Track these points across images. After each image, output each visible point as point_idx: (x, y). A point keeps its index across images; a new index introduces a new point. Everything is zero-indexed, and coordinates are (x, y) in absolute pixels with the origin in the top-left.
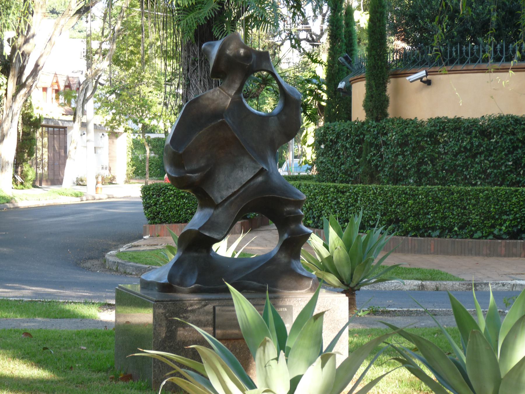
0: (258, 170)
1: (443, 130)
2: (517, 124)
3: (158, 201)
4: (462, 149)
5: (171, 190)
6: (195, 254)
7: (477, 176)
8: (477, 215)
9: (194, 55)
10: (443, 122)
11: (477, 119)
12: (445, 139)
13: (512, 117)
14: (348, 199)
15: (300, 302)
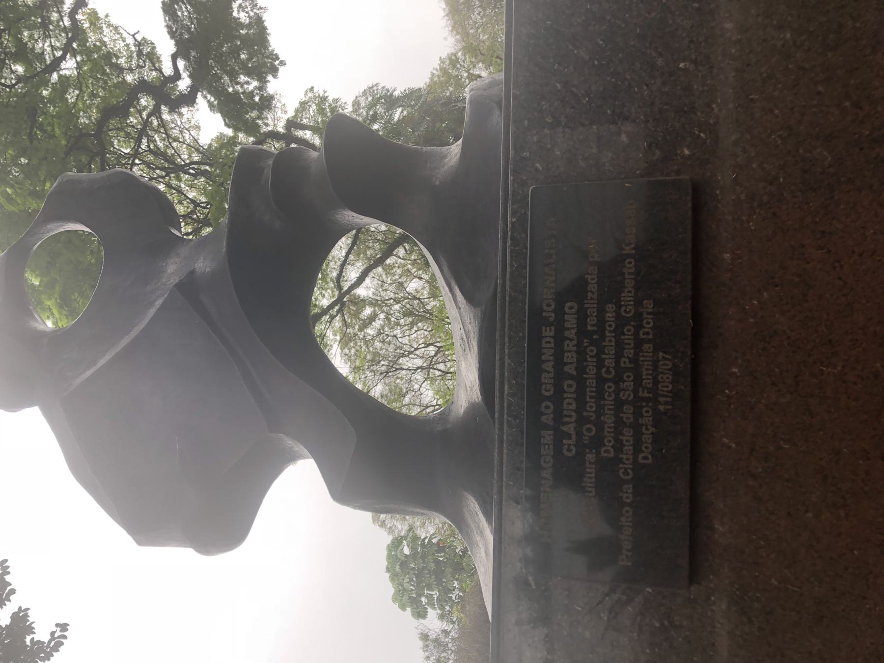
15: (526, 154)
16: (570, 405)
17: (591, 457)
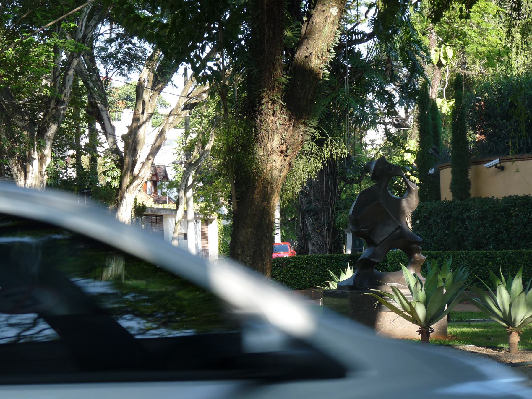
0: (397, 227)
1: (515, 206)
3: (281, 271)
4: (530, 220)
5: (292, 262)
10: (515, 199)
12: (517, 212)
14: (440, 263)
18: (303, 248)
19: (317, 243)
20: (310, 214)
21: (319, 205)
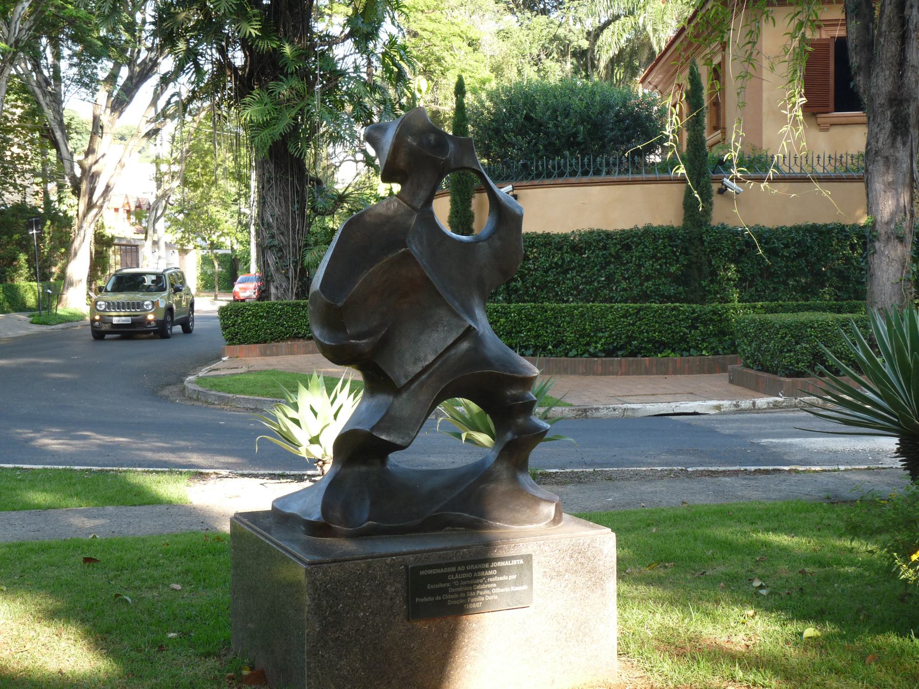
1: (532, 246)
2: (608, 238)
3: (236, 321)
5: (250, 310)
6: (363, 469)
7: (568, 292)
8: (572, 333)
9: (269, 172)
10: (533, 238)
11: (566, 234)
13: (603, 232)
15: (542, 547)
16: (464, 576)
17: (448, 585)
18: (263, 292)
19: (281, 285)
20: (273, 251)
21: (283, 240)
